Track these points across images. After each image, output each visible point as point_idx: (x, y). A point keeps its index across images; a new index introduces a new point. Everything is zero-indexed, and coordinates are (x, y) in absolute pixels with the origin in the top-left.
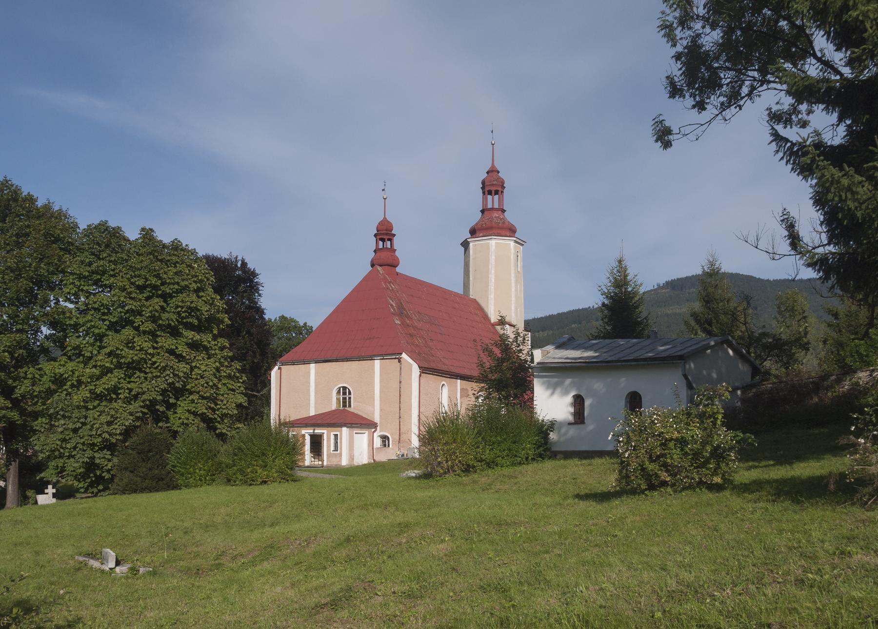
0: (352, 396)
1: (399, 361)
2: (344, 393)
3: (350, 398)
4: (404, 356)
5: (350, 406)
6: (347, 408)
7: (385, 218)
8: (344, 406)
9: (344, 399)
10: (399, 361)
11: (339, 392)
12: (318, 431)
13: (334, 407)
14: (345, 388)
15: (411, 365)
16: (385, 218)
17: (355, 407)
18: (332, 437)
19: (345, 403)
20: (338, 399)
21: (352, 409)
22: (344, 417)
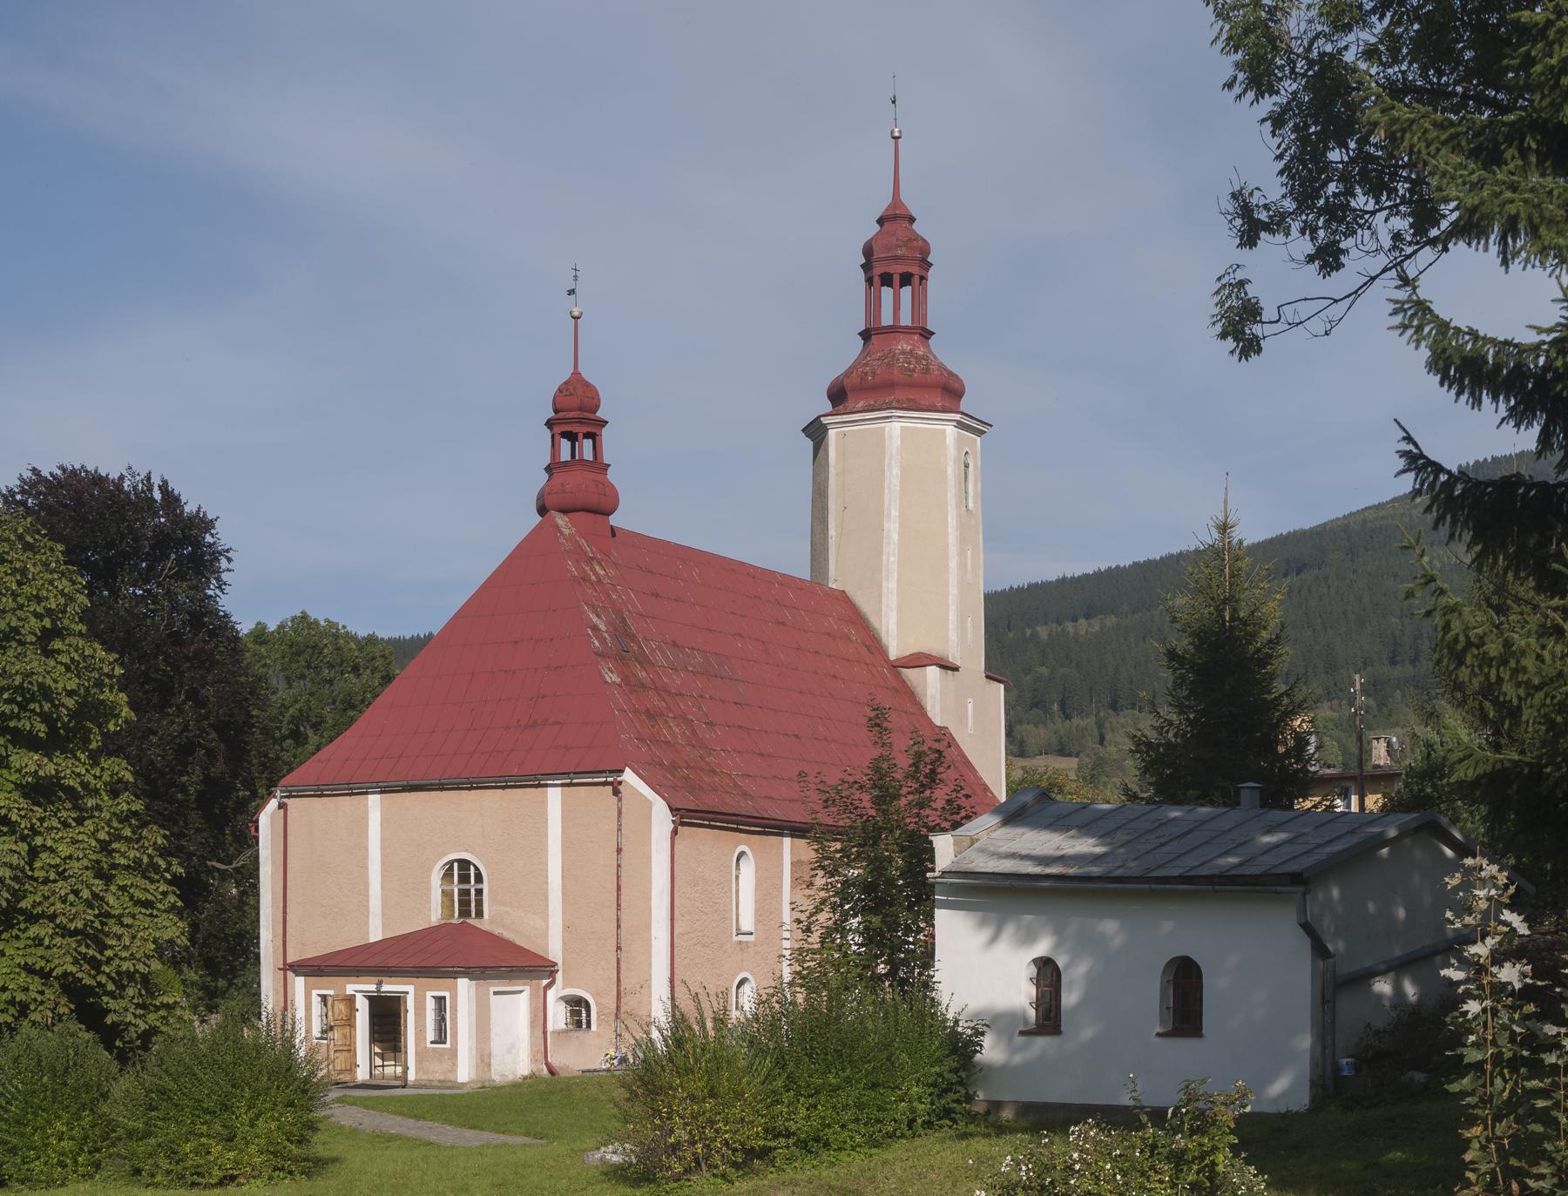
0: (485, 887)
1: (616, 792)
2: (464, 879)
3: (479, 892)
4: (629, 776)
5: (480, 914)
6: (473, 921)
7: (576, 373)
8: (465, 913)
9: (464, 893)
10: (616, 792)
11: (448, 875)
12: (390, 987)
13: (435, 916)
14: (464, 864)
15: (649, 804)
16: (576, 373)
17: (494, 917)
18: (430, 1005)
19: (465, 903)
20: (447, 895)
21: (485, 924)
22: (467, 947)
